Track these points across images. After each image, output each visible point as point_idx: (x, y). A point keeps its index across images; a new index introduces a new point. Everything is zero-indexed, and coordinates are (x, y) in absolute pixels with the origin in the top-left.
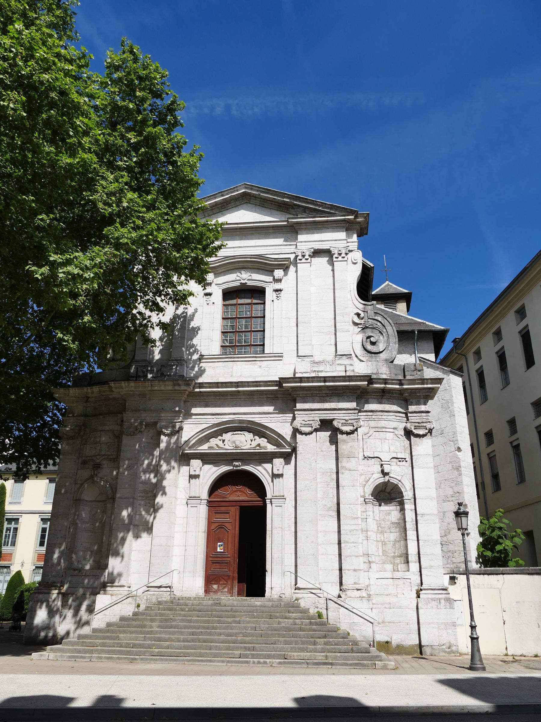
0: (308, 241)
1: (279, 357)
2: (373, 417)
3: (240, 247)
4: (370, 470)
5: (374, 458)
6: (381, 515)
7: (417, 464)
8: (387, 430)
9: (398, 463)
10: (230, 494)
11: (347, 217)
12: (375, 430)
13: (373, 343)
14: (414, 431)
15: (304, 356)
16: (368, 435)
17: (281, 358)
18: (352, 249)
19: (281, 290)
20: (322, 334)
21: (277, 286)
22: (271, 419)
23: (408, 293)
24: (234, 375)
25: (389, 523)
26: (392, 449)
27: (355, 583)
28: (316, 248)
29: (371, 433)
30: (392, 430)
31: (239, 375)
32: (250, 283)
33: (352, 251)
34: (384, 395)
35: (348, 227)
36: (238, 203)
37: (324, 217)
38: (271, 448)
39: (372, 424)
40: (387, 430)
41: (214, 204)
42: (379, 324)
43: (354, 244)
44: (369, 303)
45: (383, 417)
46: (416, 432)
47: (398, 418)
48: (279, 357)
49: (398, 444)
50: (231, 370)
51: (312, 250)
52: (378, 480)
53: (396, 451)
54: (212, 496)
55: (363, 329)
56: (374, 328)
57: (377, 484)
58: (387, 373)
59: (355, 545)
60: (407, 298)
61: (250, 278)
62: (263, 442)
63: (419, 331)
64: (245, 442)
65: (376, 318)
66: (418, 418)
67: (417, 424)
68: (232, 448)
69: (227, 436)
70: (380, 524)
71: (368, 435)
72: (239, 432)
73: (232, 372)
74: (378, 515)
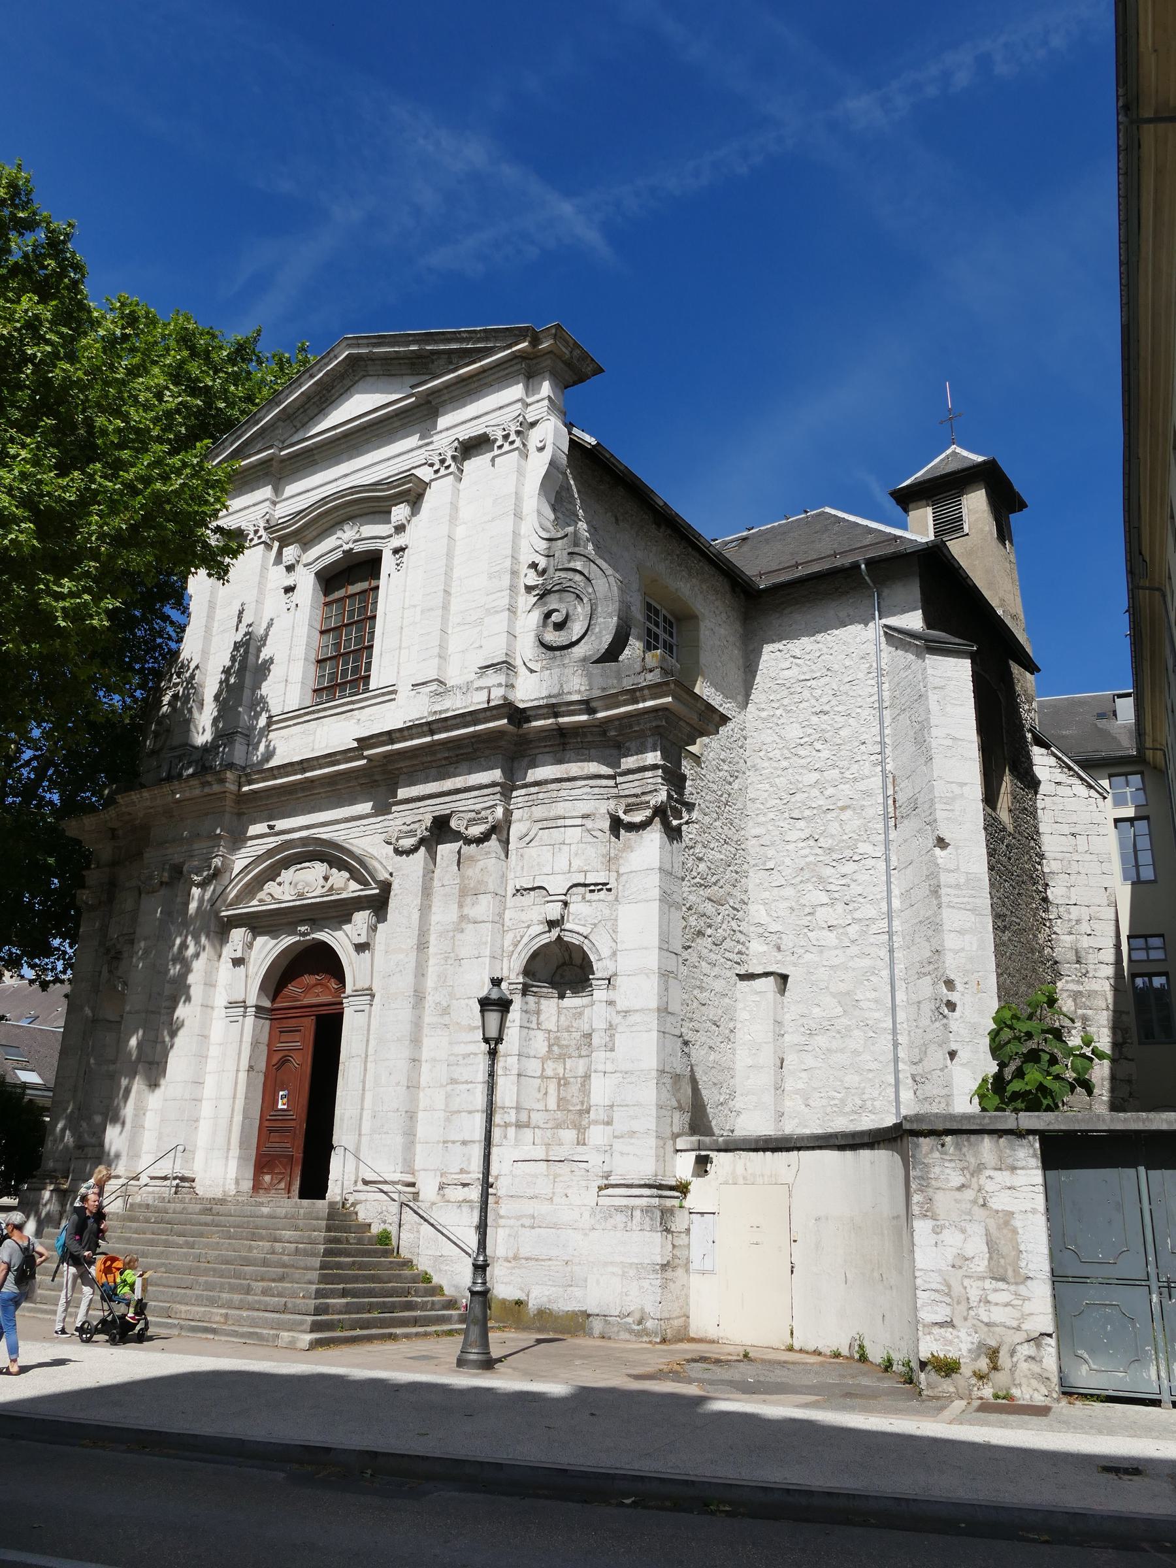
0: (457, 423)
1: (390, 693)
2: (541, 796)
4: (524, 919)
5: (533, 889)
6: (562, 1018)
7: (626, 894)
8: (568, 822)
9: (589, 896)
10: (308, 989)
12: (540, 825)
13: (559, 626)
14: (623, 816)
15: (423, 684)
16: (527, 839)
17: (393, 696)
19: (402, 549)
20: (467, 627)
21: (396, 542)
22: (364, 829)
23: (984, 462)
25: (577, 1035)
26: (577, 863)
27: (462, 1171)
30: (579, 821)
32: (359, 548)
34: (565, 743)
35: (527, 369)
36: (347, 382)
37: (474, 362)
39: (539, 812)
40: (568, 822)
41: (304, 398)
42: (578, 577)
45: (563, 793)
46: (626, 818)
47: (596, 790)
48: (390, 693)
49: (591, 852)
50: (311, 738)
52: (538, 939)
53: (585, 868)
54: (278, 999)
56: (563, 590)
57: (535, 948)
58: (583, 688)
59: (469, 1086)
60: (989, 477)
61: (357, 537)
62: (339, 878)
63: (870, 563)
64: (308, 882)
65: (572, 565)
66: (637, 783)
67: (631, 800)
69: (286, 875)
70: (557, 1038)
71: (527, 839)
72: (307, 864)
74: (554, 1019)
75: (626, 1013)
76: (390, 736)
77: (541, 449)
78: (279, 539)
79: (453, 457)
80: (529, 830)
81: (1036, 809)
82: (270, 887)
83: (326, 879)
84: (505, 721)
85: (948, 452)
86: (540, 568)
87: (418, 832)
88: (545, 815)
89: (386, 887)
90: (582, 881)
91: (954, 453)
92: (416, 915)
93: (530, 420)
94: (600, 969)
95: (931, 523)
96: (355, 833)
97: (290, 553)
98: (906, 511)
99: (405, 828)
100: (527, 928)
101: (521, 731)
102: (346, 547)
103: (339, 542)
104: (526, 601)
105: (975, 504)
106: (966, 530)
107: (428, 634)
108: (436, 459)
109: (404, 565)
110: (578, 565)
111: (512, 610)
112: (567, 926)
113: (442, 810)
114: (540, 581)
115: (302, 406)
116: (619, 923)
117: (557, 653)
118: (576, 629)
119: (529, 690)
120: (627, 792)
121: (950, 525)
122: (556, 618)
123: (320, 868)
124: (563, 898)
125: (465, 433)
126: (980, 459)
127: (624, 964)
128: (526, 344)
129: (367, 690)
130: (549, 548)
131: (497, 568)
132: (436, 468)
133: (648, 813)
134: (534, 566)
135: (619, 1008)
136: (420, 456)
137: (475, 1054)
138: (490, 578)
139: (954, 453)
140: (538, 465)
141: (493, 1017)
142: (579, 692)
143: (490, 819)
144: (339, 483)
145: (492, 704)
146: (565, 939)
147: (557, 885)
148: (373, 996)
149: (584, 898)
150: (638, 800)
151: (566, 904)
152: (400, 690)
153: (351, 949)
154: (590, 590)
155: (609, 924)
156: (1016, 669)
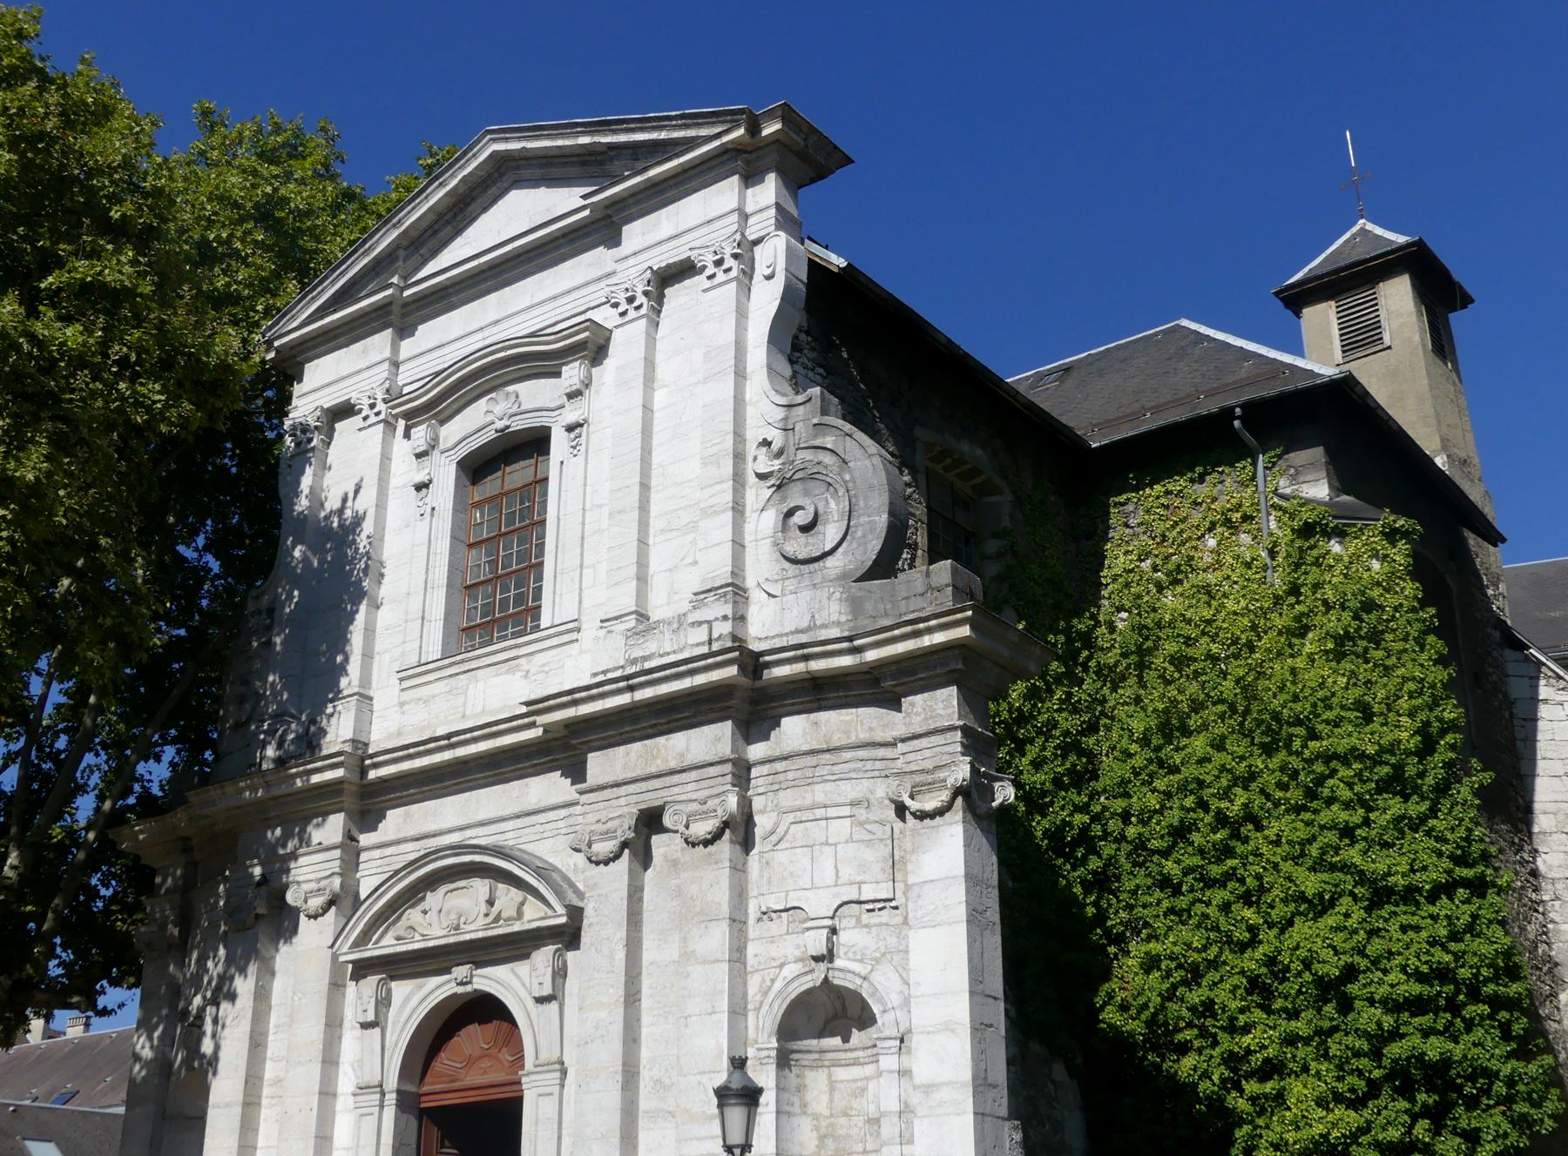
2: (790, 775)
3: (497, 322)
4: (774, 954)
5: (787, 910)
6: (837, 1096)
8: (832, 812)
9: (866, 918)
10: (470, 1062)
11: (726, 139)
12: (791, 817)
13: (806, 529)
14: (908, 802)
15: (616, 618)
16: (774, 838)
17: (574, 636)
18: (762, 234)
20: (675, 534)
21: (570, 416)
23: (1408, 245)
24: (468, 712)
25: (859, 1121)
26: (847, 872)
28: (663, 264)
29: (781, 830)
30: (846, 811)
31: (479, 710)
32: (518, 425)
35: (745, 162)
36: (493, 191)
37: (669, 159)
38: (534, 916)
39: (787, 798)
40: (832, 812)
41: (432, 217)
42: (828, 459)
44: (800, 399)
46: (913, 805)
47: (869, 765)
50: (461, 699)
51: (648, 274)
52: (795, 984)
53: (858, 879)
54: (428, 1079)
55: (779, 487)
56: (812, 477)
57: (793, 996)
58: (843, 618)
61: (515, 409)
62: (508, 897)
63: (1248, 407)
65: (817, 442)
66: (927, 753)
67: (919, 778)
69: (433, 899)
70: (831, 1125)
71: (774, 838)
74: (825, 1098)
75: (928, 1089)
76: (572, 696)
77: (769, 277)
78: (408, 416)
79: (646, 293)
80: (777, 825)
81: (1514, 740)
82: (413, 916)
83: (491, 903)
84: (732, 671)
85: (1355, 229)
86: (775, 447)
87: (619, 833)
89: (576, 914)
90: (855, 897)
91: (1363, 231)
92: (621, 955)
93: (751, 238)
94: (886, 1023)
95: (1336, 332)
96: (529, 834)
97: (420, 433)
98: (1298, 314)
99: (601, 827)
100: (782, 969)
101: (758, 684)
102: (500, 425)
103: (490, 418)
104: (757, 493)
105: (1397, 300)
106: (1387, 340)
107: (621, 546)
108: (622, 297)
109: (583, 449)
110: (829, 441)
111: (738, 509)
112: (838, 963)
113: (651, 800)
114: (776, 464)
115: (431, 227)
116: (911, 955)
117: (805, 568)
118: (830, 533)
119: (767, 624)
120: (914, 767)
121: (1362, 337)
122: (800, 518)
123: (480, 887)
124: (829, 922)
125: (663, 258)
126: (1402, 239)
127: (922, 1016)
128: (741, 131)
129: (537, 628)
130: (786, 419)
131: (715, 450)
132: (621, 309)
133: (945, 796)
134: (766, 443)
135: (917, 1080)
136: (599, 293)
138: (705, 464)
139: (1363, 231)
140: (766, 299)
141: (736, 1114)
142: (838, 624)
143: (720, 812)
144: (486, 333)
145: (716, 647)
146: (836, 982)
147: (820, 904)
148: (564, 1072)
149: (858, 919)
150: (929, 778)
151: (834, 931)
152: (584, 626)
153: (530, 1003)
154: (847, 477)
155: (896, 958)
156: (1472, 540)
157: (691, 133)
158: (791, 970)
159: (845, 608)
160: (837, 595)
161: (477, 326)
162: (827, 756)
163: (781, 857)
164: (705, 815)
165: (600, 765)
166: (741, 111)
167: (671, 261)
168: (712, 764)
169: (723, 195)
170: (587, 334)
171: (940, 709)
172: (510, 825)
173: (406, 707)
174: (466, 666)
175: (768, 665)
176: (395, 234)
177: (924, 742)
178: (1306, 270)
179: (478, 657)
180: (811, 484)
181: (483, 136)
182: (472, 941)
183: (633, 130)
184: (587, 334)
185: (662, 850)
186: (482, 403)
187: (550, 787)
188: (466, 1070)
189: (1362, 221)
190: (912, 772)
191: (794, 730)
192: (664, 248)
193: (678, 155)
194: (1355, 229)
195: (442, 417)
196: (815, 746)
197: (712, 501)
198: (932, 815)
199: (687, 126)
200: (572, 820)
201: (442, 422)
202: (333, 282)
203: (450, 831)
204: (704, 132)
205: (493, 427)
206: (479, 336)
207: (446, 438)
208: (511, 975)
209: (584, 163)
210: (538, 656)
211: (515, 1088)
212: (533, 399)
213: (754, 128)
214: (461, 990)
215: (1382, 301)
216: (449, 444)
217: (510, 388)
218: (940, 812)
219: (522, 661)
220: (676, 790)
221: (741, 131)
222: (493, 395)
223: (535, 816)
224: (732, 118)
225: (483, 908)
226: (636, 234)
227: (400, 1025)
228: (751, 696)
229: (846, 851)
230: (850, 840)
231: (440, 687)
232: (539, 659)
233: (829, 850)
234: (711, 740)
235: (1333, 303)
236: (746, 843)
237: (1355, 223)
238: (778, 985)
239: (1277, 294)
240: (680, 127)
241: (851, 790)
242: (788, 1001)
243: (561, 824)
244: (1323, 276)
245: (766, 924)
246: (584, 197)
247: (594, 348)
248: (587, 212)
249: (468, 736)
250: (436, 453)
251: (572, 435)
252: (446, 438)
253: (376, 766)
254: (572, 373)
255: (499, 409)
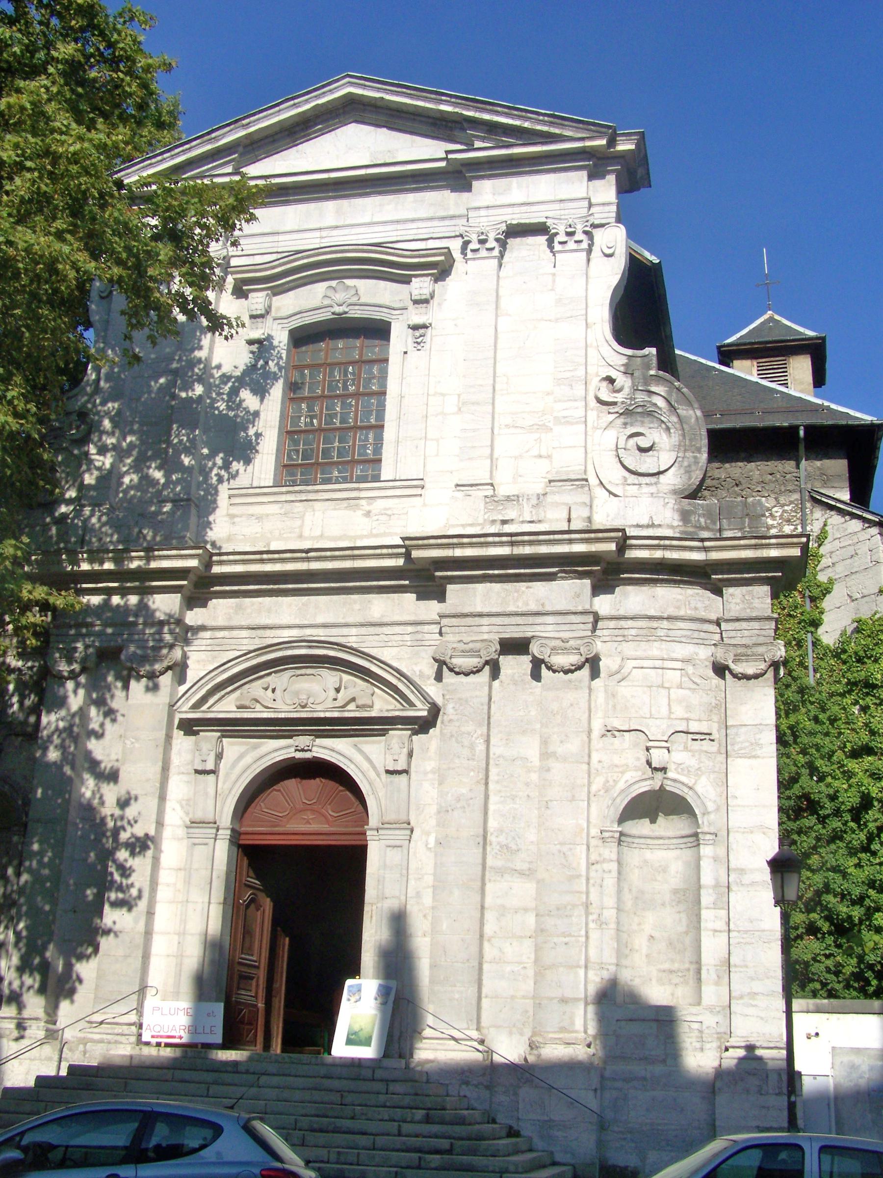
1: (415, 486)
3: (337, 227)
7: (736, 747)
11: (588, 143)
14: (732, 666)
15: (472, 485)
16: (619, 676)
17: (418, 491)
18: (604, 221)
19: (425, 327)
21: (417, 316)
22: (386, 638)
23: (817, 338)
24: (306, 533)
26: (679, 711)
27: (563, 1030)
28: (515, 222)
29: (625, 671)
30: (678, 665)
31: (318, 533)
33: (602, 226)
35: (596, 164)
38: (383, 705)
43: (607, 208)
46: (738, 668)
47: (696, 635)
48: (415, 486)
49: (695, 699)
50: (298, 523)
51: (503, 227)
52: (636, 786)
53: (686, 716)
56: (650, 414)
57: (634, 794)
59: (566, 940)
60: (816, 351)
61: (354, 300)
63: (808, 428)
64: (321, 693)
66: (746, 633)
67: (740, 650)
68: (291, 708)
69: (280, 680)
73: (301, 526)
80: (621, 667)
82: (255, 688)
84: (613, 547)
85: (766, 317)
88: (639, 653)
89: (435, 711)
91: (771, 319)
99: (461, 646)
102: (338, 309)
103: (327, 302)
109: (427, 346)
115: (272, 136)
117: (632, 479)
122: (644, 443)
126: (811, 333)
129: (376, 478)
133: (763, 666)
137: (574, 906)
142: (672, 527)
146: (668, 788)
148: (412, 831)
152: (427, 486)
157: (553, 130)
158: (631, 776)
159: (677, 516)
160: (671, 505)
161: (317, 226)
162: (665, 622)
163: (624, 690)
164: (566, 651)
165: (463, 596)
166: (609, 127)
167: (523, 221)
168: (575, 613)
169: (572, 185)
170: (442, 258)
171: (756, 603)
172: (354, 631)
173: (236, 520)
174: (303, 497)
175: (631, 547)
176: (242, 133)
177: (744, 625)
178: (738, 335)
179: (317, 491)
180: (647, 420)
181: (344, 78)
182: (281, 719)
183: (497, 113)
184: (442, 258)
185: (509, 672)
186: (321, 287)
187: (407, 605)
188: (302, 819)
189: (770, 312)
190: (735, 645)
191: (632, 599)
192: (517, 210)
193: (543, 143)
194: (766, 317)
195: (276, 290)
196: (652, 613)
197: (565, 413)
198: (748, 677)
199: (551, 124)
200: (419, 636)
201: (275, 295)
202: (172, 157)
203: (289, 627)
204: (568, 133)
205: (333, 310)
206: (317, 234)
207: (278, 309)
208: (353, 751)
209: (434, 125)
210: (379, 501)
211: (362, 837)
212: (371, 296)
213: (612, 142)
214: (299, 755)
215: (790, 370)
216: (279, 315)
217: (349, 282)
218: (756, 677)
219: (363, 502)
220: (538, 628)
221: (603, 142)
222: (334, 283)
223: (395, 630)
224: (598, 130)
225: (332, 693)
226: (486, 190)
227: (233, 777)
228: (609, 567)
229: (676, 693)
230: (680, 687)
231: (274, 509)
232: (380, 504)
233: (664, 692)
234: (569, 592)
235: (755, 363)
236: (595, 673)
237: (765, 313)
238: (621, 785)
239: (719, 348)
240: (544, 123)
241: (682, 650)
242: (629, 798)
243: (407, 638)
244: (745, 344)
245: (609, 739)
246: (447, 152)
247: (442, 270)
248: (443, 164)
249: (328, 554)
250: (269, 318)
251: (417, 333)
252: (278, 309)
253: (221, 563)
254: (421, 285)
255: (340, 297)
